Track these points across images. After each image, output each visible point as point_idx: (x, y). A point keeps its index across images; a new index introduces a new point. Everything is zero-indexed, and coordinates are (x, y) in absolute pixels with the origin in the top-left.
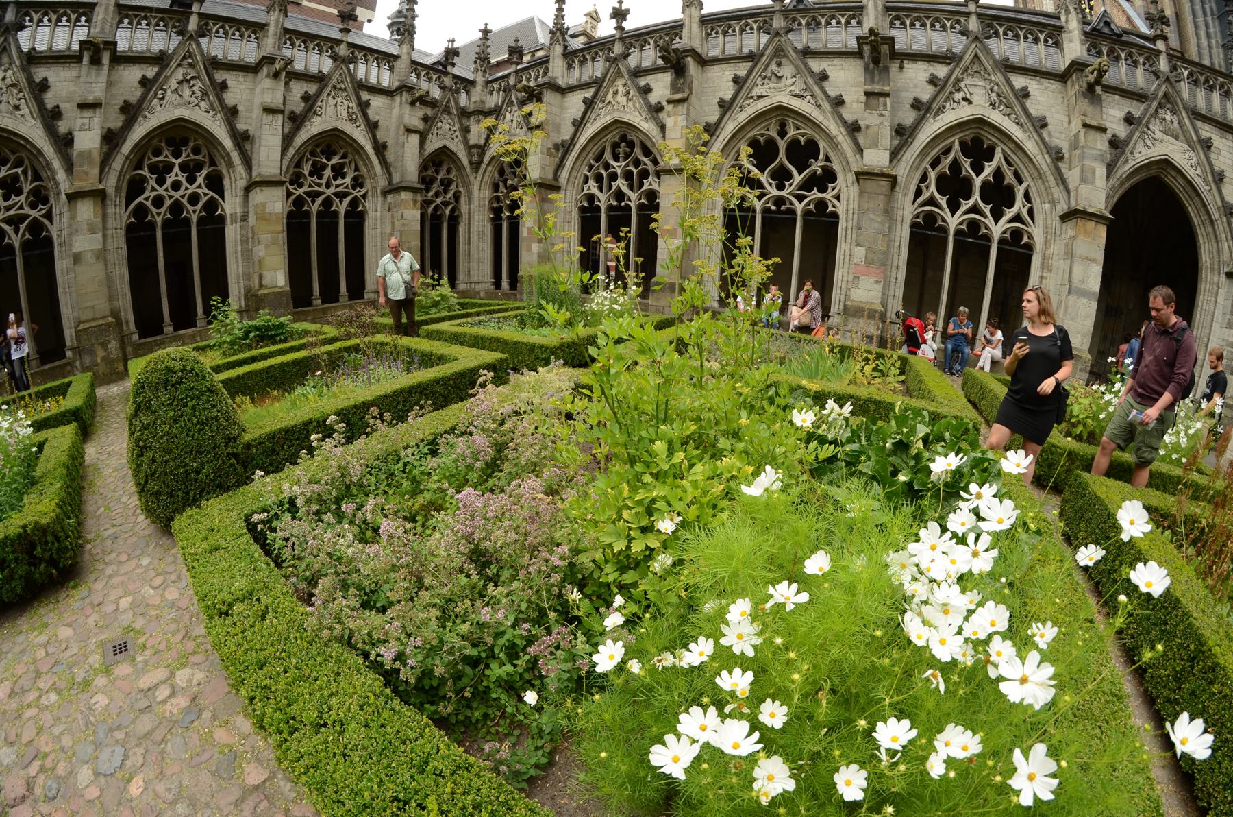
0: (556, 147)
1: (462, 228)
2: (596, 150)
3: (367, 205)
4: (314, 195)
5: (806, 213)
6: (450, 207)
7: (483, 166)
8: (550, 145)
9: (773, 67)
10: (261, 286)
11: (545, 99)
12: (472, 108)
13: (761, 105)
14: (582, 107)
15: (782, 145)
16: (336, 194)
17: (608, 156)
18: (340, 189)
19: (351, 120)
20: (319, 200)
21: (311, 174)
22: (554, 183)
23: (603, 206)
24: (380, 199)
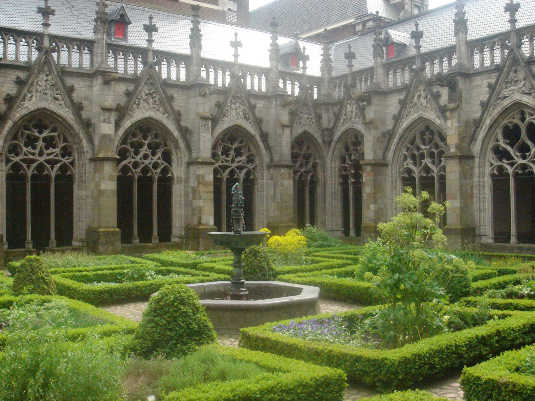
0: (384, 135)
1: (319, 190)
2: (410, 137)
3: (256, 174)
4: (224, 168)
6: (310, 174)
7: (333, 144)
9: (512, 74)
10: (200, 223)
13: (506, 103)
14: (398, 106)
15: (523, 127)
17: (418, 141)
20: (228, 170)
21: (222, 154)
22: (383, 162)
23: (416, 175)
24: (266, 172)
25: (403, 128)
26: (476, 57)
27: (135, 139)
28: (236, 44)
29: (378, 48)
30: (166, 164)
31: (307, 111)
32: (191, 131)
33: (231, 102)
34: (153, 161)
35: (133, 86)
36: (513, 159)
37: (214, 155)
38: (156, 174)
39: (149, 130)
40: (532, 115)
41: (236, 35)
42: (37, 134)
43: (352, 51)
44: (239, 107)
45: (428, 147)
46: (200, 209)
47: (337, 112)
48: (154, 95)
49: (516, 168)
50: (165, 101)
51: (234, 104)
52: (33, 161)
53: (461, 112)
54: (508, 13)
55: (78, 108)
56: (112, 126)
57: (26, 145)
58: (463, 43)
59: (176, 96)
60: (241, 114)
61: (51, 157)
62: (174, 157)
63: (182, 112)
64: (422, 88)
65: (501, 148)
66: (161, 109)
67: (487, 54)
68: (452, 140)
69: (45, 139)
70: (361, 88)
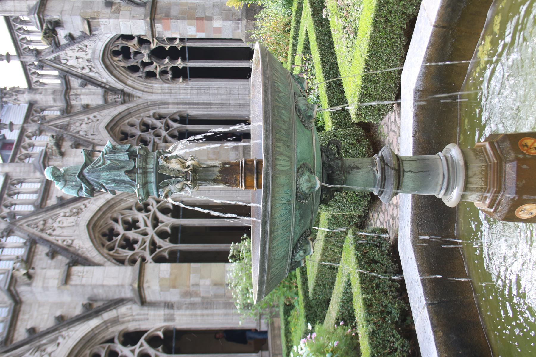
1: (193, 112)
4: (154, 246)
6: (171, 123)
7: (127, 89)
8: (108, 11)
11: (56, 17)
12: (61, 104)
16: (155, 226)
18: (149, 223)
19: (78, 213)
20: (159, 241)
21: (133, 249)
22: (149, 7)
30: (142, 340)
31: (78, 124)
32: (90, 299)
33: (50, 235)
37: (133, 262)
44: (59, 222)
46: (215, 285)
47: (80, 81)
50: (36, 343)
51: (54, 230)
60: (72, 219)
62: (132, 327)
63: (58, 314)
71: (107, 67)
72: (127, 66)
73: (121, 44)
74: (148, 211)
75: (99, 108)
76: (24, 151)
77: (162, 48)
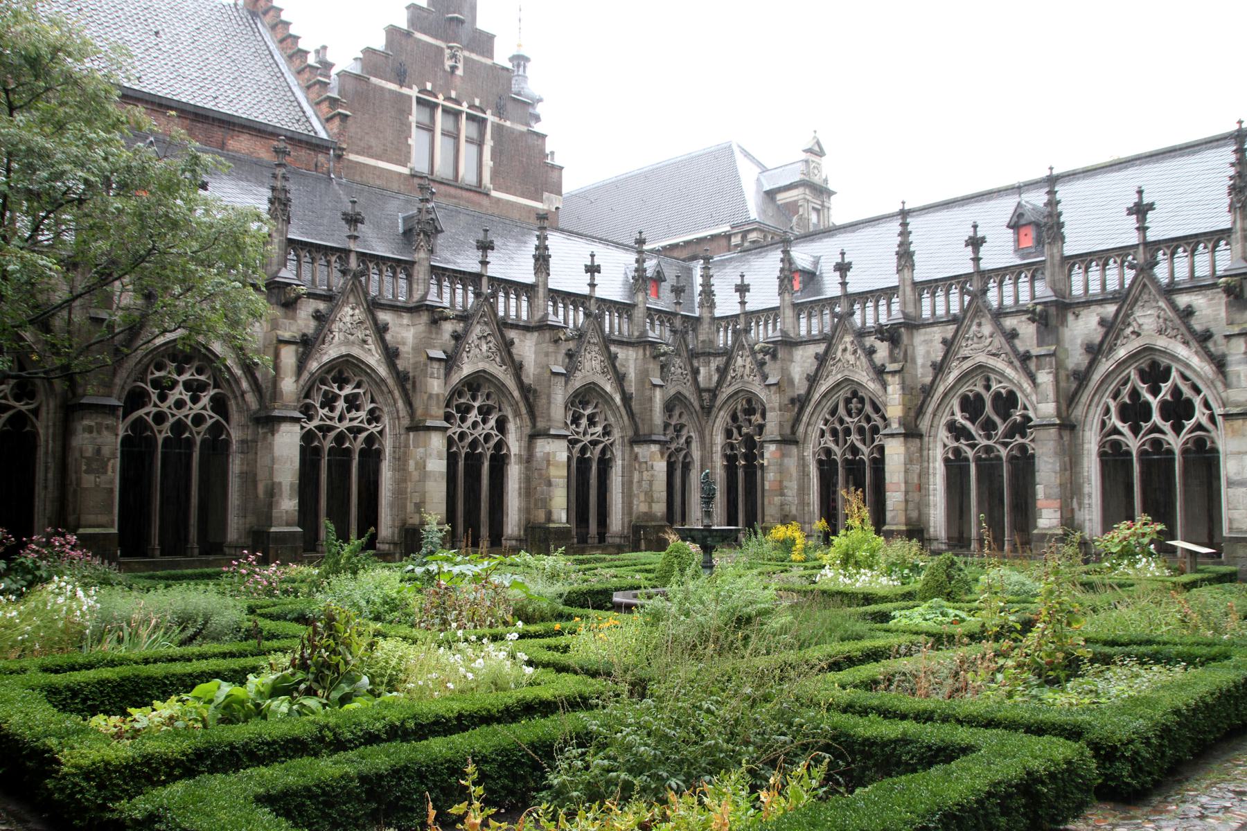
0: (793, 401)
2: (829, 405)
4: (575, 442)
5: (1012, 459)
7: (715, 410)
11: (779, 356)
12: (699, 349)
13: (966, 365)
16: (590, 442)
17: (841, 411)
18: (594, 437)
20: (579, 446)
23: (838, 459)
25: (821, 392)
26: (926, 302)
27: (462, 401)
28: (593, 269)
29: (786, 281)
30: (500, 436)
32: (535, 391)
34: (485, 432)
35: (462, 325)
36: (973, 438)
38: (487, 451)
39: (478, 389)
40: (1000, 382)
41: (592, 256)
42: (337, 391)
43: (746, 282)
45: (856, 420)
48: (489, 338)
49: (978, 451)
52: (330, 429)
53: (906, 375)
54: (970, 248)
55: (391, 355)
56: (442, 381)
57: (322, 407)
58: (908, 282)
59: (516, 341)
61: (355, 423)
64: (848, 339)
65: (958, 425)
66: (498, 359)
67: (940, 300)
68: (894, 409)
69: (347, 399)
70: (761, 334)
71: (736, 393)
72: (738, 411)
73: (758, 407)
74: (604, 435)
75: (695, 380)
76: (656, 317)
77: (755, 447)
